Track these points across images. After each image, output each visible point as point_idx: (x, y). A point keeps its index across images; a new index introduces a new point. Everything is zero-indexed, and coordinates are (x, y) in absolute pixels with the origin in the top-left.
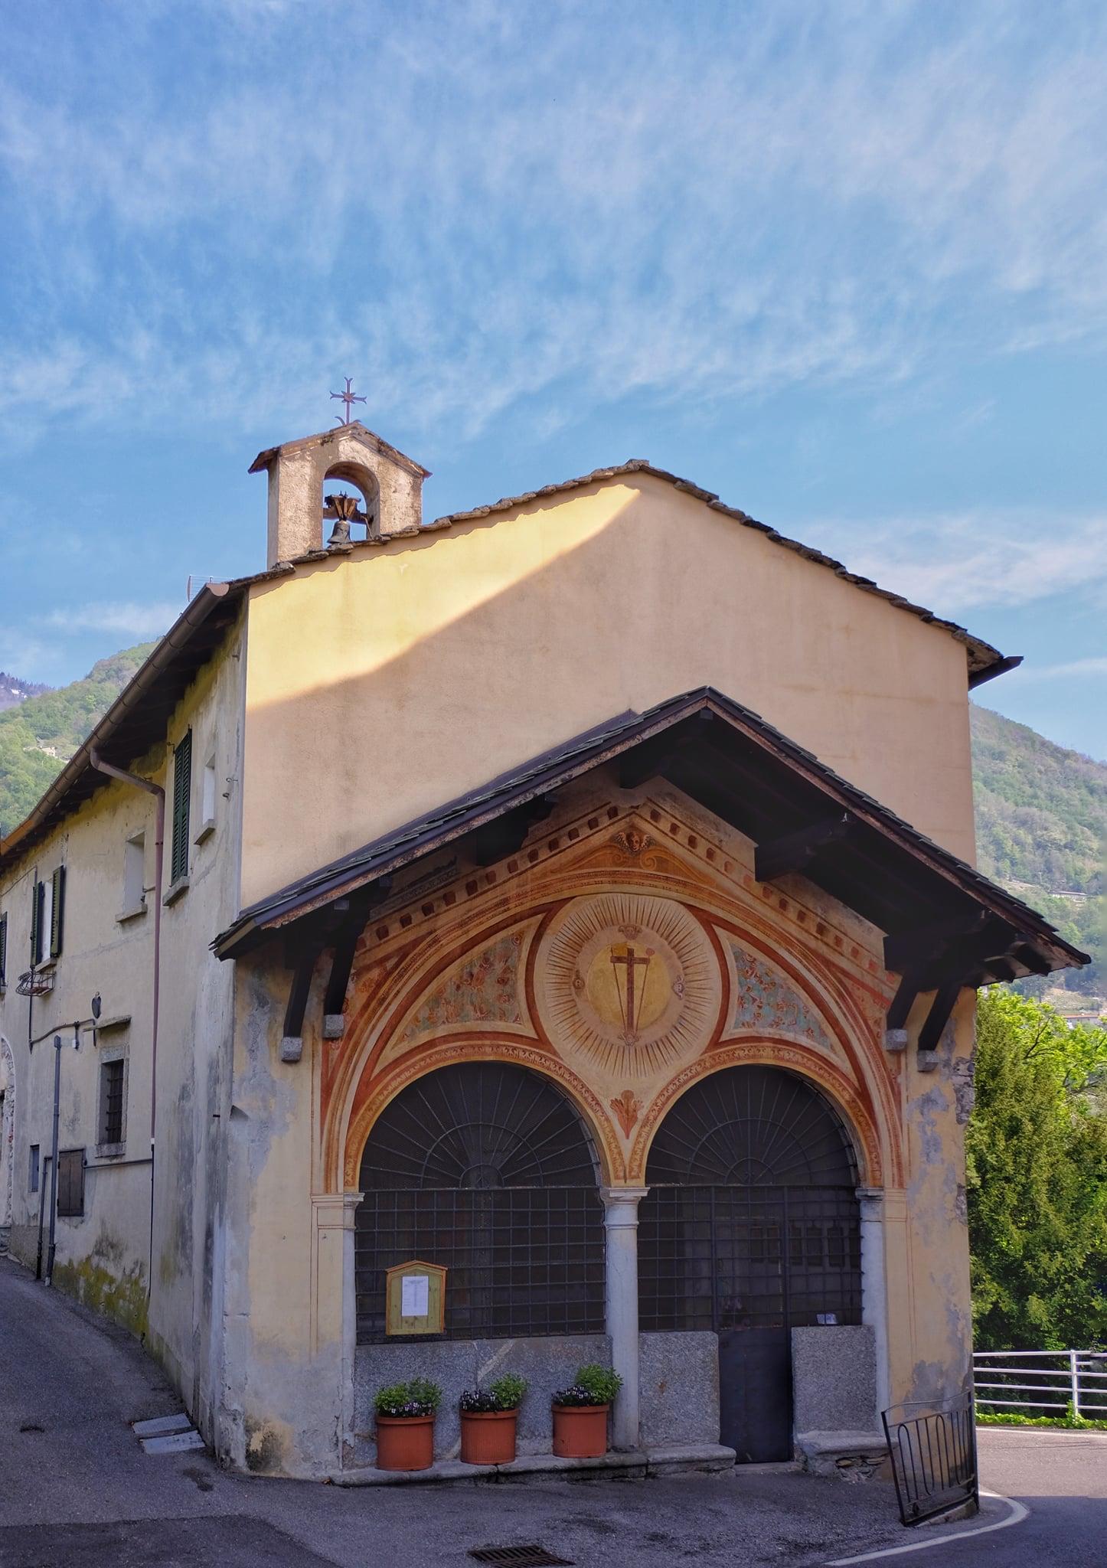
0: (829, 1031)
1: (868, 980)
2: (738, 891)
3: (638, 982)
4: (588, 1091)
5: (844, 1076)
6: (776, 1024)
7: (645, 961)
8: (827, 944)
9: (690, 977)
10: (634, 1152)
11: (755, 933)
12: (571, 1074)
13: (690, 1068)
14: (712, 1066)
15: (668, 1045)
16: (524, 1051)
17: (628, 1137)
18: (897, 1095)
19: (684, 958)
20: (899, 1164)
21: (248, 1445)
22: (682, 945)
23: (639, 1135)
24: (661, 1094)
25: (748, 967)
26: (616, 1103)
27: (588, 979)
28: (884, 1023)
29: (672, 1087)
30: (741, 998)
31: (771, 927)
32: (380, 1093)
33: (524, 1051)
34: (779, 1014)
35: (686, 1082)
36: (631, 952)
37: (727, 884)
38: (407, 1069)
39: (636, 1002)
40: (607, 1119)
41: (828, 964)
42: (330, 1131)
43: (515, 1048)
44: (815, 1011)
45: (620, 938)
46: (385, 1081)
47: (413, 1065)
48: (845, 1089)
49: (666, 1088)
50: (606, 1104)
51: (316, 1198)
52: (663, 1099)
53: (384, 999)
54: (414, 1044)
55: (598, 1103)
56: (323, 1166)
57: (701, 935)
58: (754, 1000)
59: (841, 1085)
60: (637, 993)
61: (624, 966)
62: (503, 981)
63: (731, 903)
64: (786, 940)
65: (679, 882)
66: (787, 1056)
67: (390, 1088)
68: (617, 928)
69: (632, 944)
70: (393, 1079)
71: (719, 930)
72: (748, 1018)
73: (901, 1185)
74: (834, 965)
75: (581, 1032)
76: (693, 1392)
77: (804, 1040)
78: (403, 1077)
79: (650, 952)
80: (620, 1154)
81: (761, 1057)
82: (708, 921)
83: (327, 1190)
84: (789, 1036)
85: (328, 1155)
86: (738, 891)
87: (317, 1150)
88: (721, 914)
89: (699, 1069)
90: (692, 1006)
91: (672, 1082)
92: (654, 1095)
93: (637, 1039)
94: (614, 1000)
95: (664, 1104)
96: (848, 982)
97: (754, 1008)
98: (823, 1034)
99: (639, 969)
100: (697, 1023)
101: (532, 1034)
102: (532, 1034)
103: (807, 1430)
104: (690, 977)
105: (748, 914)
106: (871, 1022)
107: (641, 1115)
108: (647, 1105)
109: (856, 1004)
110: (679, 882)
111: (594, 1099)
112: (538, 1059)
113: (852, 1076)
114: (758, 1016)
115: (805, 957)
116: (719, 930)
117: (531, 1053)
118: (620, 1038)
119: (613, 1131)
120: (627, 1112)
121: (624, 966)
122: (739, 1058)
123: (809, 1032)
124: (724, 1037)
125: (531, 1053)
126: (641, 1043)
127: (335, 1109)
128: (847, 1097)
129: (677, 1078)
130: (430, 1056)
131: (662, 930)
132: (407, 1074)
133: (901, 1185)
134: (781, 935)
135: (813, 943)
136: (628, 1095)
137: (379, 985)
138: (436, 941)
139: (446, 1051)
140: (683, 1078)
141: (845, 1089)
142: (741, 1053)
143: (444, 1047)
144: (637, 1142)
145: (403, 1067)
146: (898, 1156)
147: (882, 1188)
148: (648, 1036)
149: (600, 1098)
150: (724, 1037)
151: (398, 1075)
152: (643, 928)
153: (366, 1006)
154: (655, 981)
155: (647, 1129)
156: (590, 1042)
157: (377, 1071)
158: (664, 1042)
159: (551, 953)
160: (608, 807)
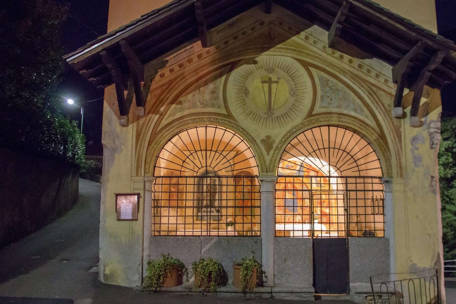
0: (365, 109)
1: (384, 87)
2: (320, 52)
3: (273, 91)
4: (250, 136)
5: (373, 129)
6: (339, 107)
7: (277, 82)
8: (363, 72)
9: (297, 88)
10: (271, 161)
11: (328, 69)
12: (243, 129)
13: (297, 126)
14: (308, 125)
15: (287, 116)
16: (222, 120)
17: (268, 155)
18: (399, 137)
19: (295, 80)
20: (401, 167)
21: (104, 271)
22: (294, 75)
23: (274, 154)
24: (284, 137)
25: (325, 83)
26: (263, 141)
27: (251, 90)
28: (393, 105)
29: (289, 134)
30: (322, 97)
31: (336, 66)
32: (160, 137)
33: (222, 120)
34: (340, 102)
35: (296, 132)
36: (270, 79)
37: (315, 49)
38: (172, 128)
39: (273, 99)
40: (259, 147)
41: (364, 81)
42: (139, 152)
43: (217, 119)
44: (358, 101)
45: (266, 73)
46: (163, 133)
47: (174, 126)
48: (373, 134)
49: (286, 134)
50: (258, 141)
51: (133, 178)
52: (285, 139)
53: (162, 101)
54: (175, 118)
55: (255, 141)
56: (136, 166)
57: (302, 71)
58: (328, 97)
59: (371, 132)
60: (273, 96)
61: (267, 85)
62: (213, 92)
63: (316, 57)
64: (344, 72)
65: (291, 50)
66: (344, 120)
67: (164, 135)
68: (264, 69)
69: (271, 76)
70: (166, 132)
71: (311, 69)
72: (325, 104)
73: (401, 176)
74: (367, 81)
75: (247, 112)
76: (300, 263)
77: (353, 113)
78: (170, 131)
79: (279, 78)
80: (265, 162)
81: (332, 121)
82: (306, 65)
83: (137, 175)
84: (345, 112)
85: (138, 161)
86: (320, 52)
87: (133, 160)
88: (312, 62)
89: (302, 126)
90: (299, 100)
91: (289, 132)
92: (280, 138)
93: (273, 114)
94: (262, 98)
95: (285, 141)
96: (374, 89)
97: (328, 100)
98: (362, 111)
99: (274, 86)
100: (301, 107)
101: (226, 113)
102: (226, 113)
103: (355, 282)
104: (297, 88)
105: (324, 61)
106: (386, 105)
107: (275, 146)
108: (277, 141)
109: (378, 98)
110: (291, 50)
111: (253, 139)
112: (228, 123)
113: (377, 129)
114: (329, 104)
115: (353, 78)
116: (311, 69)
117: (225, 120)
118: (265, 113)
119: (261, 152)
120: (268, 144)
121: (267, 85)
122: (321, 121)
123: (355, 110)
124: (314, 113)
125: (225, 120)
126: (275, 116)
127: (141, 144)
128: (374, 138)
129: (292, 130)
130: (181, 123)
131: (284, 69)
132: (172, 130)
133: (401, 176)
134: (340, 69)
135: (356, 72)
136: (268, 137)
137: (160, 95)
138: (184, 77)
139: (188, 120)
140: (294, 130)
141: (373, 134)
142: (322, 119)
143: (187, 119)
144: (273, 157)
145: (170, 127)
146: (400, 163)
147: (392, 177)
148: (277, 113)
149: (256, 139)
150: (314, 113)
151: (168, 130)
152: (276, 69)
153: (155, 103)
154: (282, 92)
155: (277, 152)
156: (251, 116)
157: (159, 129)
158: (286, 115)
159: (235, 80)
160: (260, 22)
